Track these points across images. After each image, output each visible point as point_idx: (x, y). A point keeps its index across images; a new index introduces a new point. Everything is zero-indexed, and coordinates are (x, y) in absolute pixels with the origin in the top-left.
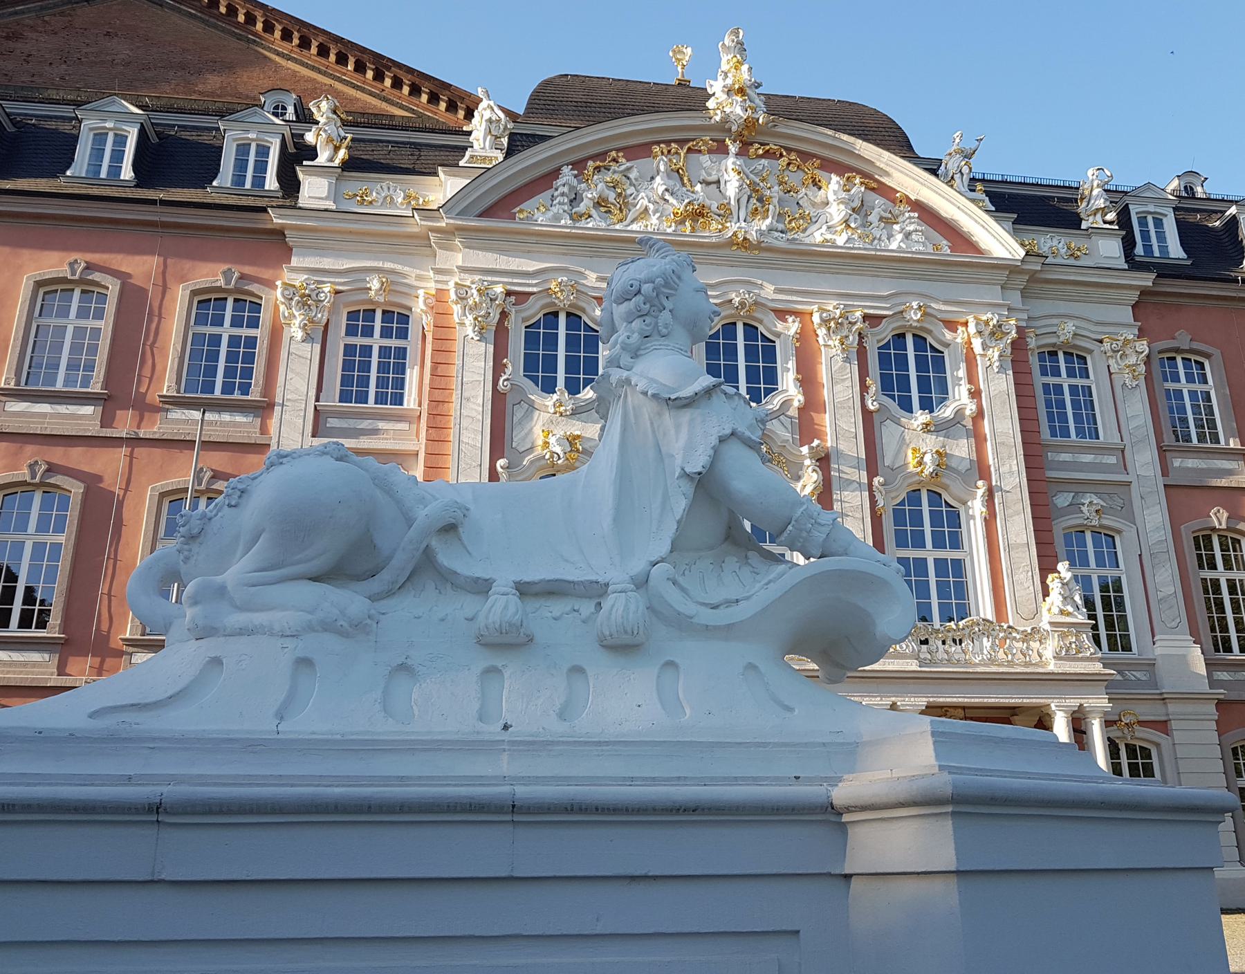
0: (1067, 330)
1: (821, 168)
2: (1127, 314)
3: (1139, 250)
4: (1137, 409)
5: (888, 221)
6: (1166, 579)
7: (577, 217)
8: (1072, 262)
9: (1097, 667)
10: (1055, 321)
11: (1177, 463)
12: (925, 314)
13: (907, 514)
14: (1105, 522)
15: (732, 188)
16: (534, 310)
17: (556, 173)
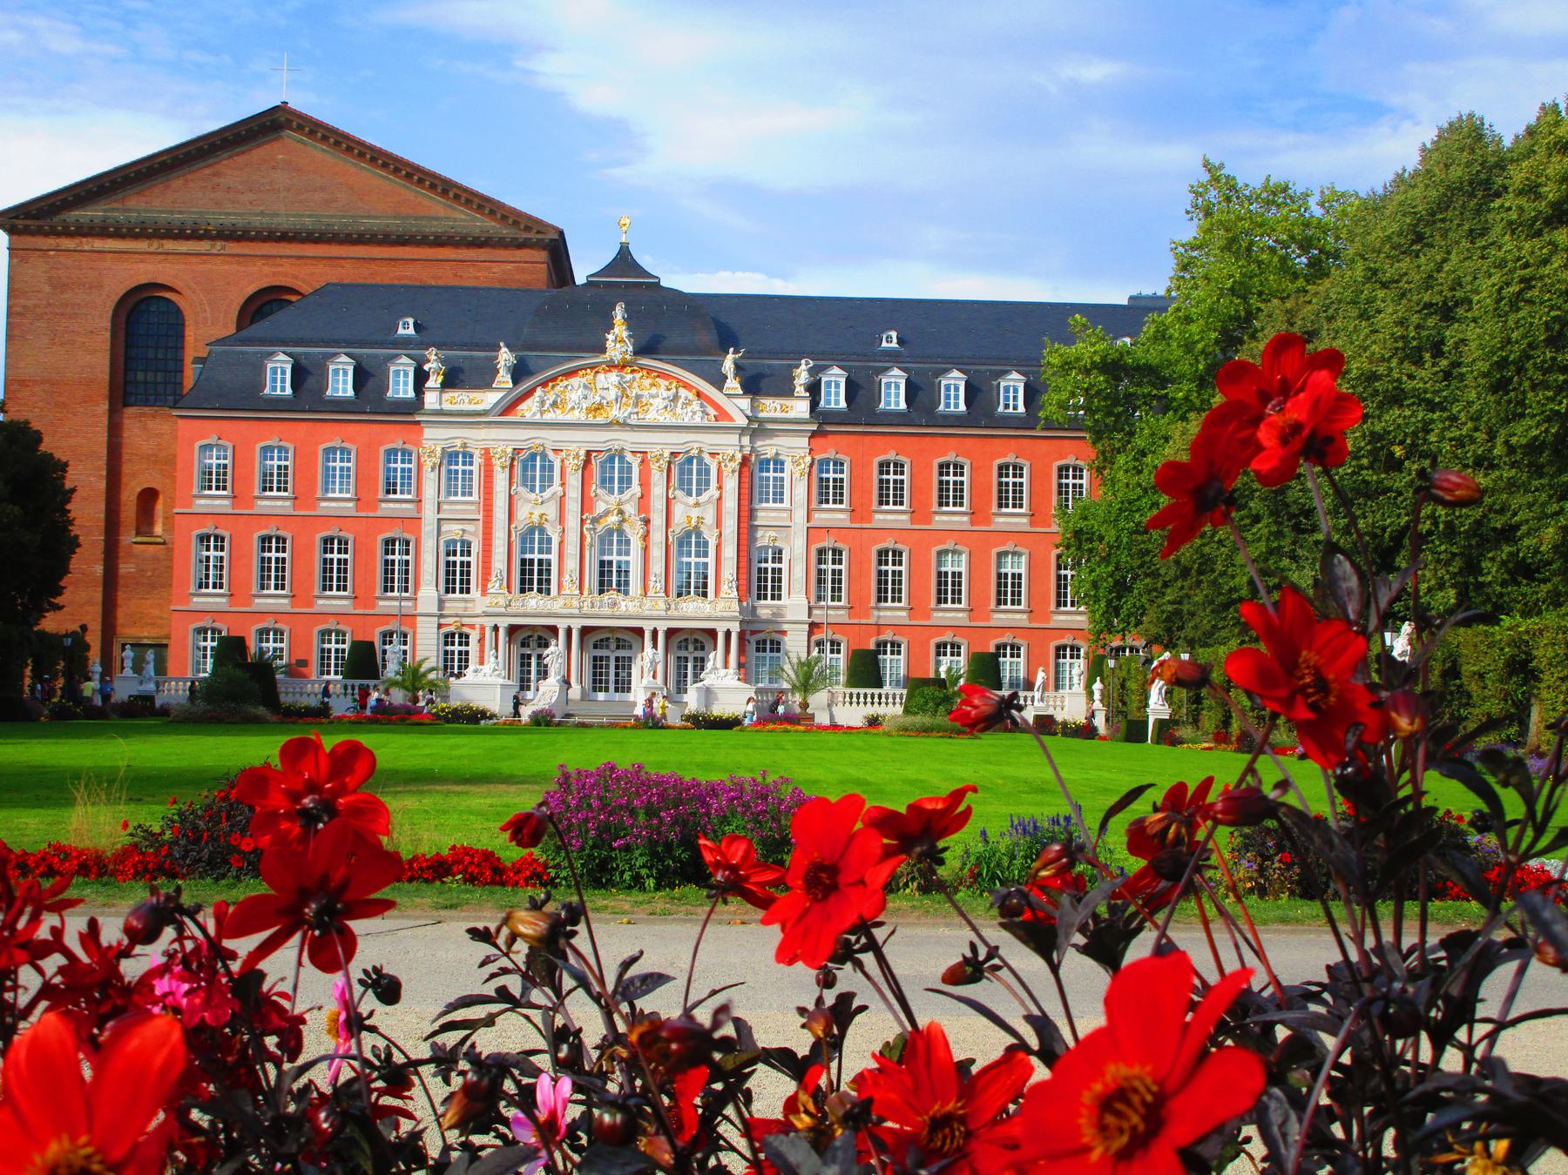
2: (804, 442)
3: (822, 403)
4: (801, 490)
5: (688, 403)
6: (799, 571)
7: (542, 413)
8: (784, 415)
11: (817, 515)
12: (701, 451)
13: (684, 541)
15: (612, 394)
16: (524, 455)
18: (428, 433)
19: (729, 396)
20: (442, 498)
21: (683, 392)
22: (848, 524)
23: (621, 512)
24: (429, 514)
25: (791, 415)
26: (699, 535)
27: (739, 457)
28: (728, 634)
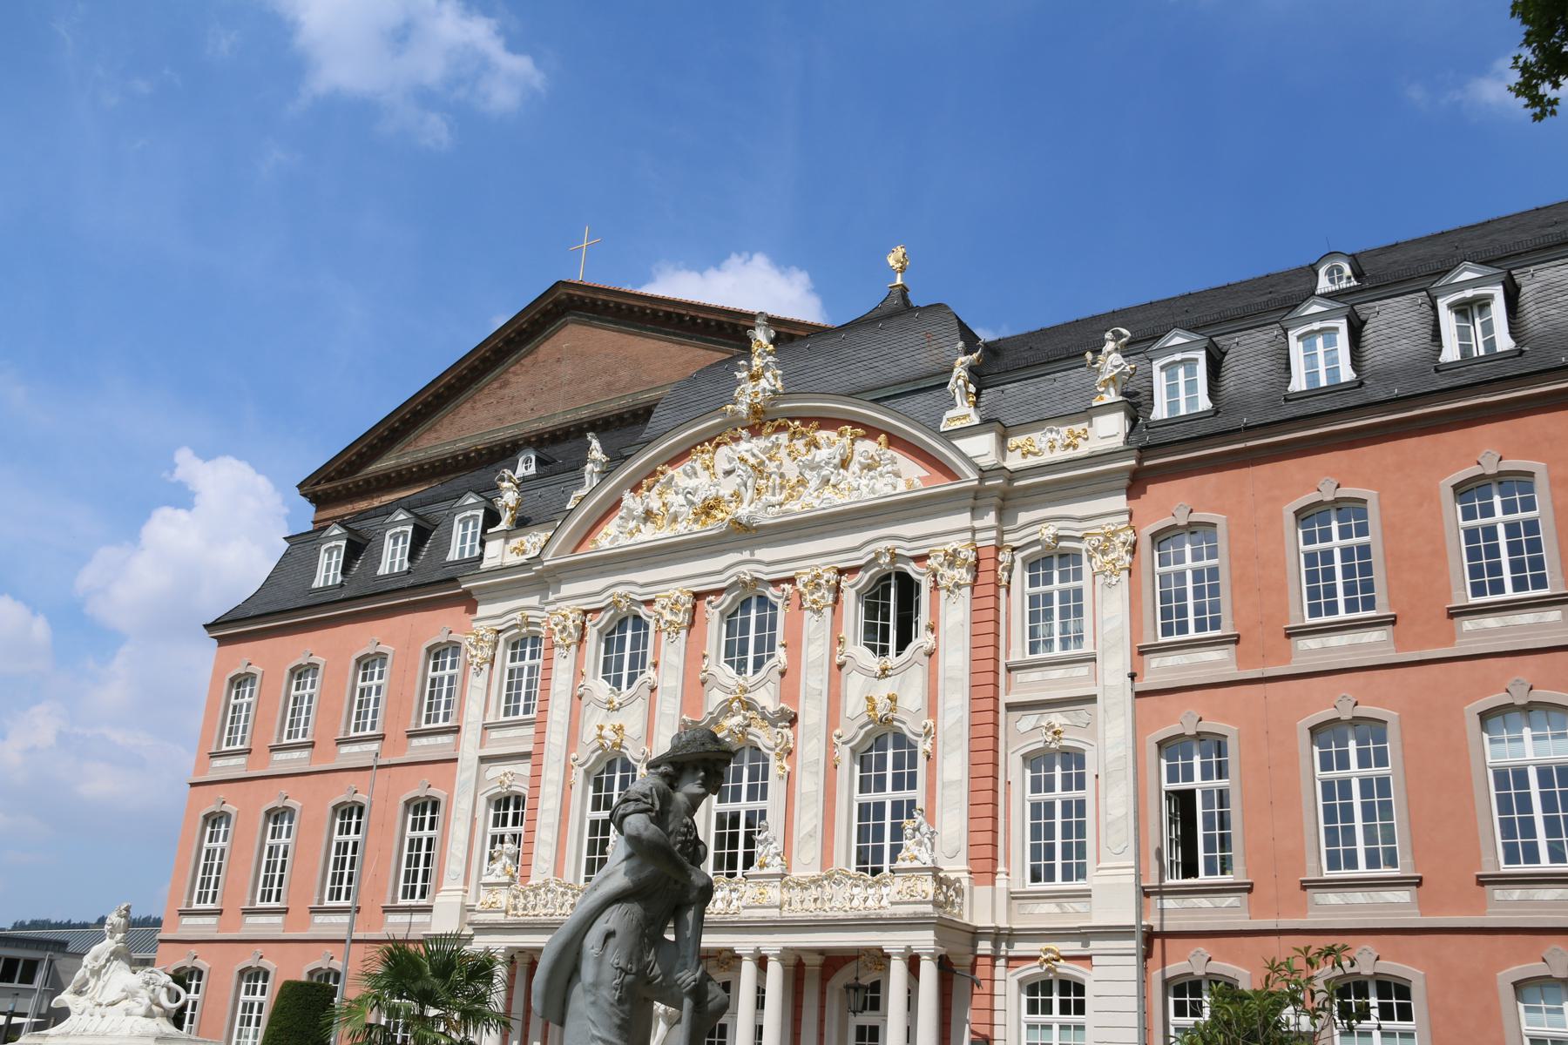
0: (1048, 532)
1: (821, 427)
3: (1160, 412)
8: (1070, 454)
9: (929, 908)
10: (1037, 528)
14: (1065, 743)
17: (621, 500)
18: (482, 610)
19: (948, 437)
20: (490, 719)
21: (867, 447)
22: (1234, 673)
23: (748, 706)
24: (469, 747)
25: (1084, 449)
26: (900, 740)
27: (968, 555)
28: (913, 963)
